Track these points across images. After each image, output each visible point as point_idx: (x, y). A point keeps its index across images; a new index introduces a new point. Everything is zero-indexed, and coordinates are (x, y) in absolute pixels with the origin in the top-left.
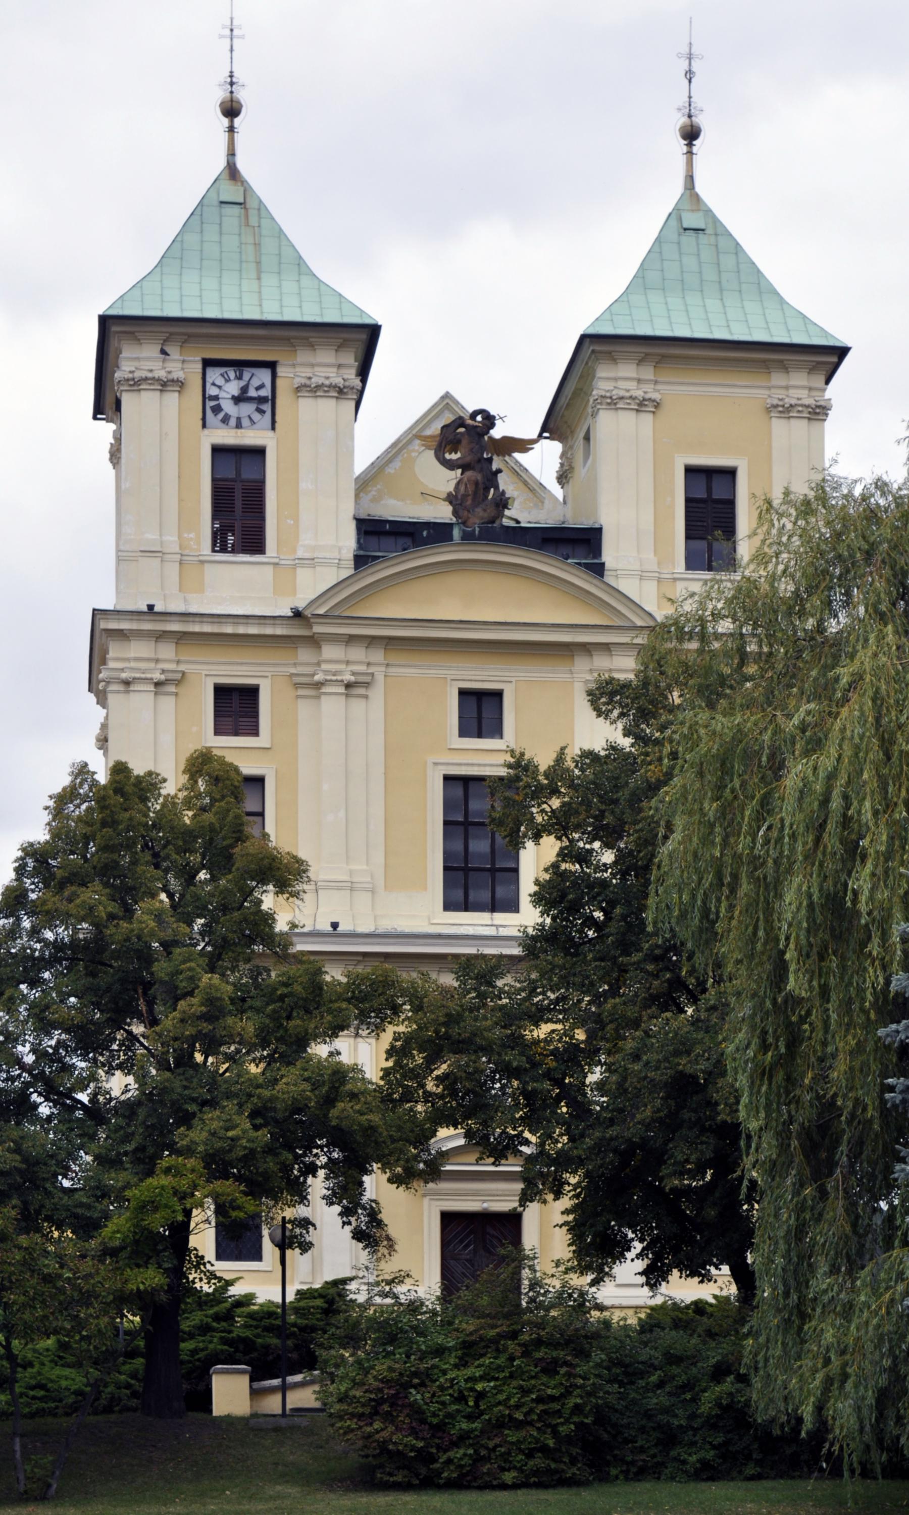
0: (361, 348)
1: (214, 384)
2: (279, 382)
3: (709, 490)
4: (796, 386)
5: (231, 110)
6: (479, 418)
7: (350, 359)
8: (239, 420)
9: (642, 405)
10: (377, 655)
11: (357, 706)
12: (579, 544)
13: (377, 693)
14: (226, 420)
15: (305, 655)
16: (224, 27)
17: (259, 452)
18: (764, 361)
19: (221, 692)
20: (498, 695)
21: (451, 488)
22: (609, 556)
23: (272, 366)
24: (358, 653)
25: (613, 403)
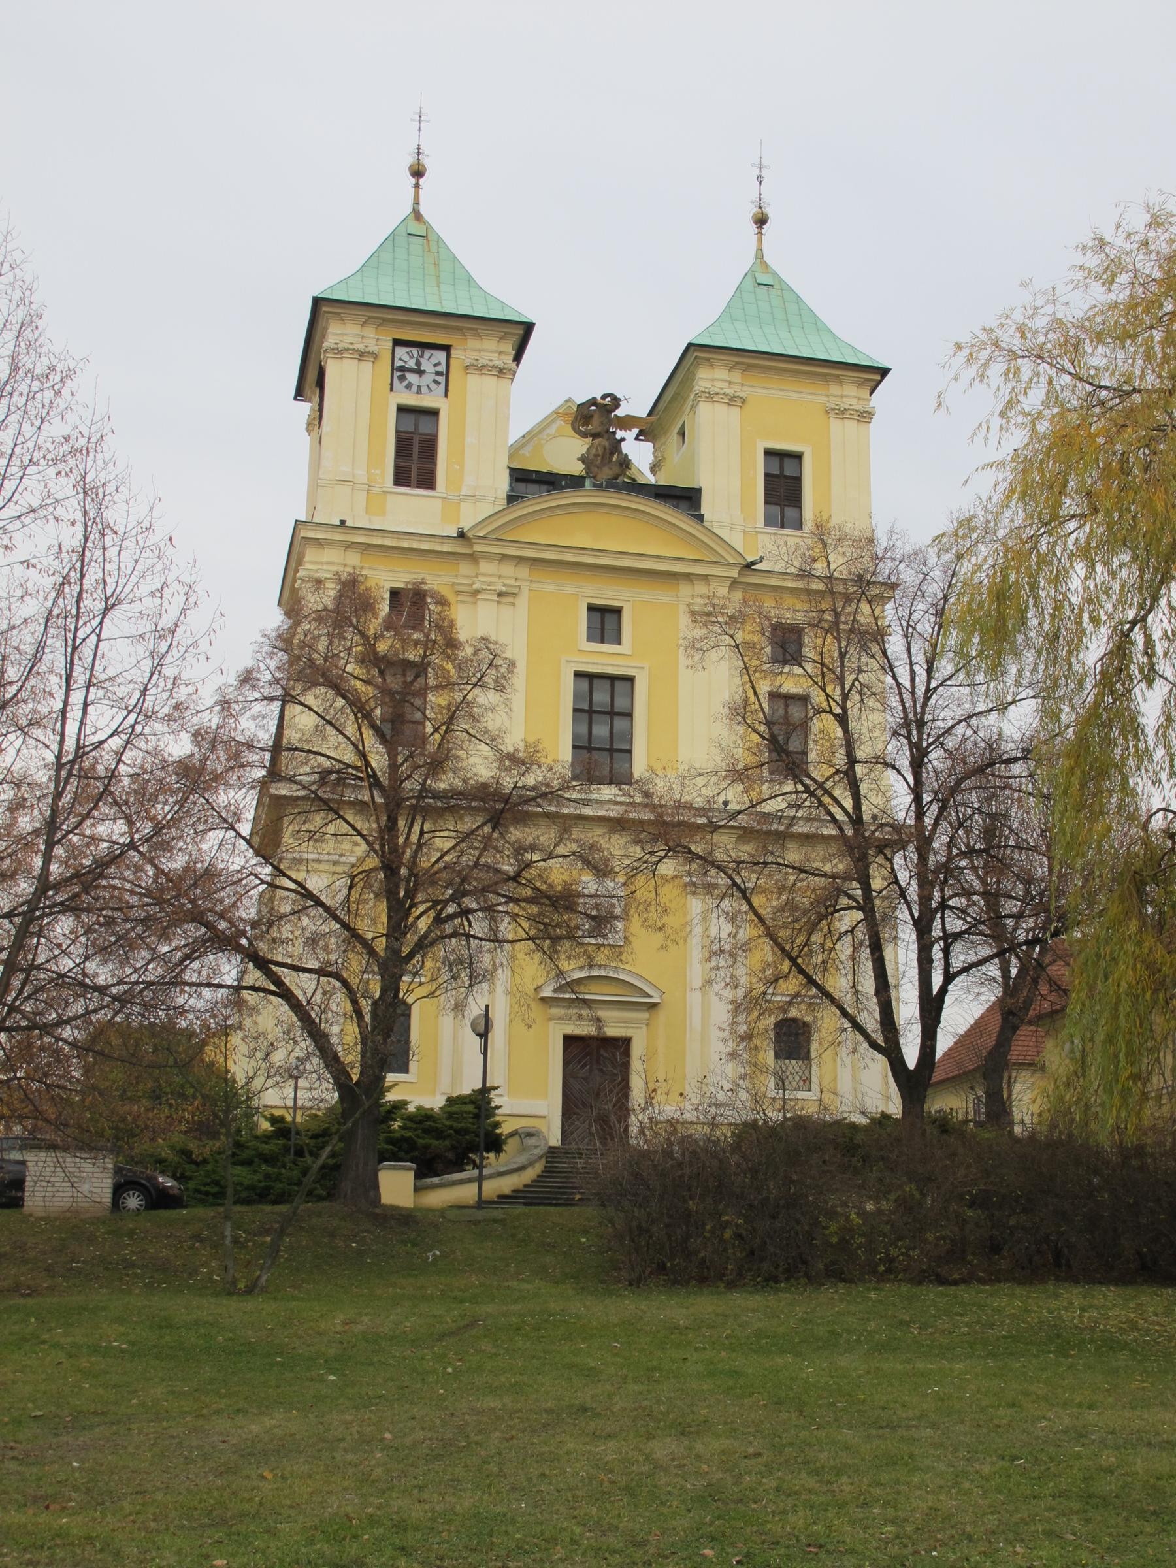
0: (516, 339)
2: (452, 361)
3: (782, 468)
4: (849, 394)
5: (418, 173)
6: (608, 399)
7: (509, 348)
8: (419, 387)
9: (732, 400)
10: (523, 572)
11: (506, 611)
12: (686, 499)
13: (522, 602)
14: (409, 386)
15: (465, 568)
16: (415, 113)
17: (434, 413)
18: (825, 375)
20: (617, 611)
21: (584, 451)
22: (705, 509)
23: (447, 348)
24: (508, 569)
25: (711, 397)
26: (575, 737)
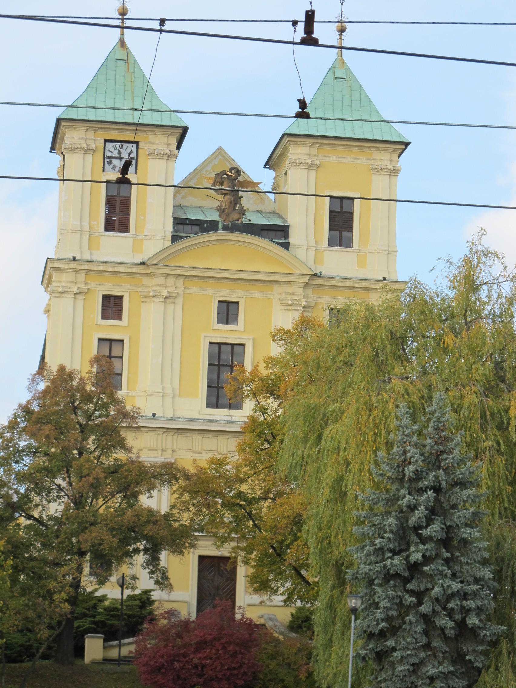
1: (109, 151)
2: (140, 151)
3: (341, 207)
4: (383, 158)
6: (233, 171)
7: (173, 141)
11: (170, 307)
12: (279, 233)
13: (180, 301)
19: (106, 298)
23: (137, 143)
24: (171, 281)
25: (296, 165)
26: (209, 381)
